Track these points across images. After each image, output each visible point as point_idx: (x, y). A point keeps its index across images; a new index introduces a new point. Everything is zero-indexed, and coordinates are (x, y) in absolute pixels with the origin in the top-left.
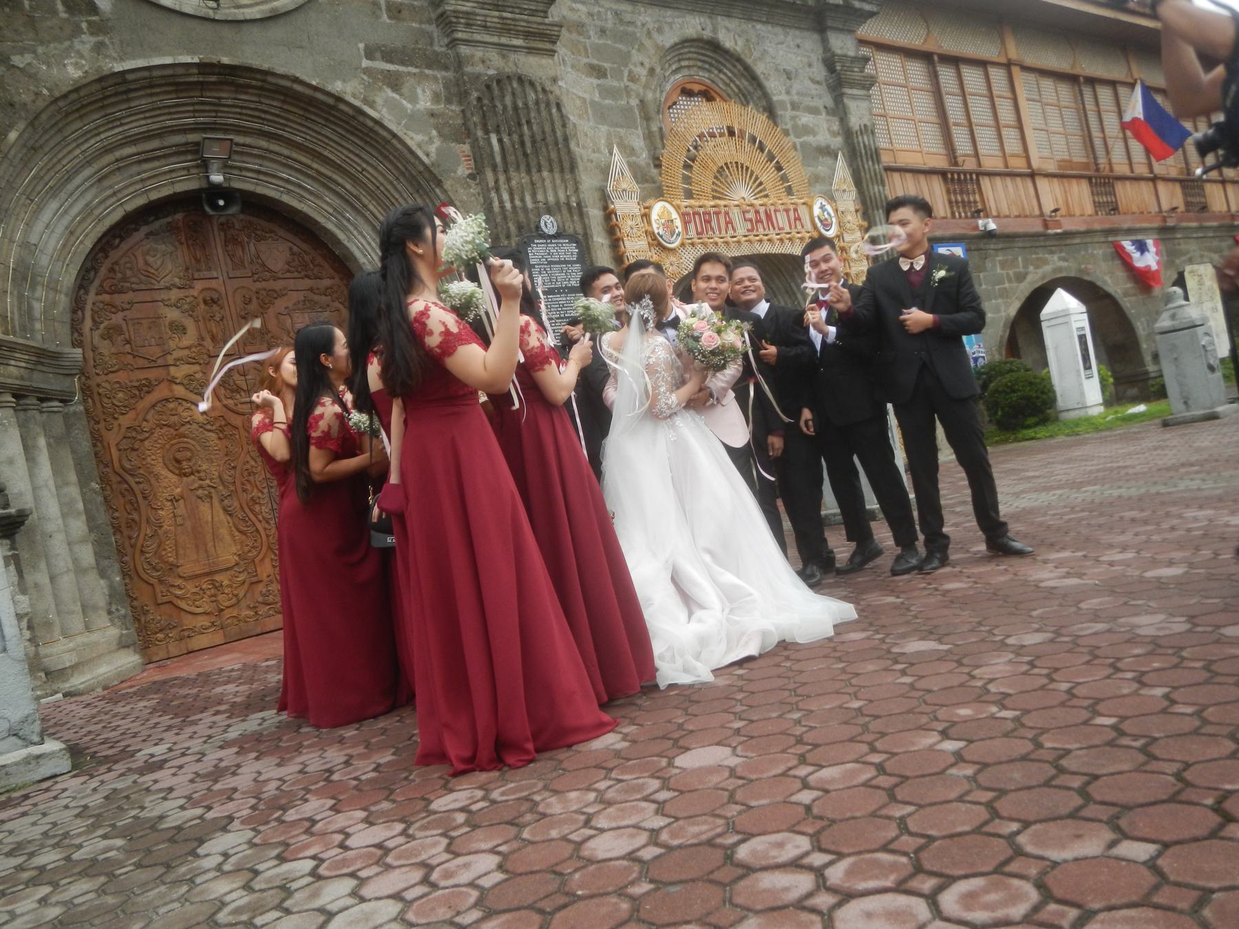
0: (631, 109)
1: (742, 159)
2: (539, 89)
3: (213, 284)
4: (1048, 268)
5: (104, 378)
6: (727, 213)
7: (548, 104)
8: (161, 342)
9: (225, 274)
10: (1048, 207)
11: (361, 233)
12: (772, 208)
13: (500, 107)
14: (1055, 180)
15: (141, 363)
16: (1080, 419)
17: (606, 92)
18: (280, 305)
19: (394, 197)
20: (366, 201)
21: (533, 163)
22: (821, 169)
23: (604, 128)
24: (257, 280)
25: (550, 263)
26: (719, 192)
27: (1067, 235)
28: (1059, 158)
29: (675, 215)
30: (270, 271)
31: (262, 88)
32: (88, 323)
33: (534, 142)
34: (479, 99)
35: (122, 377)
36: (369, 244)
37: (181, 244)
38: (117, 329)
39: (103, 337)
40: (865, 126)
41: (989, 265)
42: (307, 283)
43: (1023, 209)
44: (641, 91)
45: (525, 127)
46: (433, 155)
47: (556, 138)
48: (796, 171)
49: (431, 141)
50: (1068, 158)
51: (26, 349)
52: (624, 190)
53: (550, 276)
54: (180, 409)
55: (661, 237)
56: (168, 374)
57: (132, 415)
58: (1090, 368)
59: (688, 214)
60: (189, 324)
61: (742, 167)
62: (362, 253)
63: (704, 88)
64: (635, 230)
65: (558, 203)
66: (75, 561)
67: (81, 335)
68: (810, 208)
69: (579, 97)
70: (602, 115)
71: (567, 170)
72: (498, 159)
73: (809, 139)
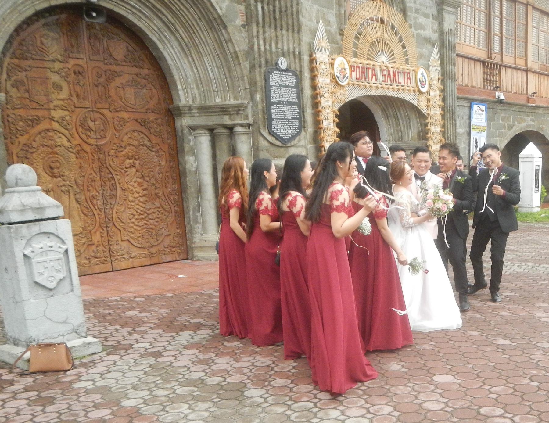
1: (386, 38)
3: (80, 62)
4: (524, 124)
5: (12, 111)
6: (374, 70)
8: (47, 95)
9: (88, 57)
10: (531, 91)
11: (172, 46)
12: (397, 70)
14: (537, 75)
15: (35, 105)
16: (528, 213)
18: (118, 81)
19: (196, 29)
21: (278, 25)
22: (425, 51)
23: (316, 7)
24: (106, 64)
25: (281, 86)
26: (371, 56)
27: (537, 107)
28: (540, 63)
29: (347, 67)
33: (280, 12)
35: (22, 112)
36: (176, 54)
37: (64, 34)
38: (22, 82)
39: (13, 86)
40: (451, 30)
41: (496, 118)
42: (135, 70)
43: (519, 89)
46: (224, 9)
47: (292, 11)
48: (412, 50)
50: (545, 63)
52: (322, 47)
53: (280, 93)
54: (56, 137)
56: (50, 115)
57: (26, 136)
58: (538, 187)
60: (64, 84)
61: (385, 43)
62: (171, 57)
65: (288, 50)
68: (416, 73)
71: (296, 32)
73: (421, 32)
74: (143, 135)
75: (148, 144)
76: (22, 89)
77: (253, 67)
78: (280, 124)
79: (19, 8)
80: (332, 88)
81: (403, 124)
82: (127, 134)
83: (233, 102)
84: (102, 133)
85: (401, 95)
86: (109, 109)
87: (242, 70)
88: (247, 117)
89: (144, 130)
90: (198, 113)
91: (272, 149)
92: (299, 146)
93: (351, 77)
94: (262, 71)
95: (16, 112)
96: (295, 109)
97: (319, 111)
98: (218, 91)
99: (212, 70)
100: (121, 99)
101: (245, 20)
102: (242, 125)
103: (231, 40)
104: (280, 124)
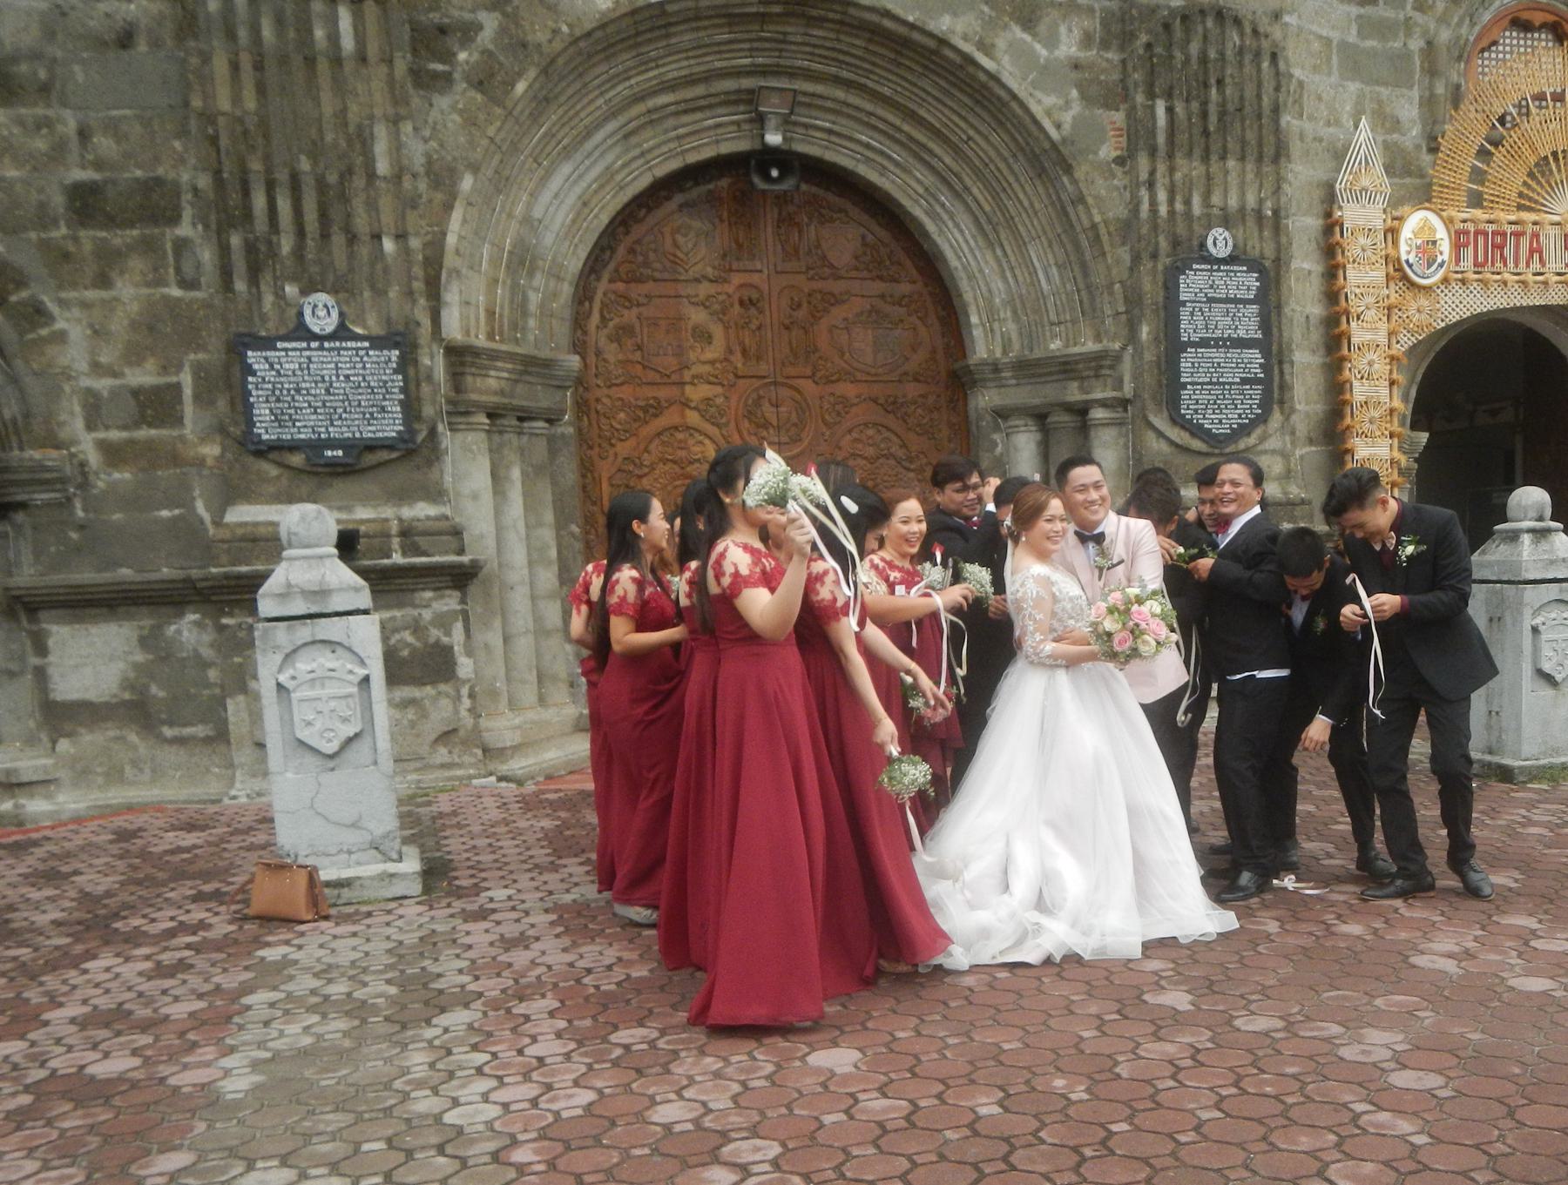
0: (1406, 56)
2: (1248, 30)
3: (755, 279)
5: (605, 391)
6: (1536, 236)
7: (1258, 55)
8: (680, 352)
13: (1179, 56)
15: (652, 376)
17: (1367, 27)
20: (968, 182)
21: (1215, 147)
23: (1353, 87)
24: (812, 278)
25: (1211, 300)
26: (1530, 199)
29: (1441, 234)
30: (832, 266)
32: (595, 318)
33: (1222, 114)
34: (1149, 46)
35: (625, 392)
37: (722, 221)
38: (627, 330)
39: (611, 339)
44: (1432, 26)
45: (1214, 91)
46: (1067, 127)
49: (1068, 105)
55: (1410, 266)
57: (632, 442)
59: (1467, 233)
60: (717, 331)
63: (1551, 18)
64: (1369, 253)
65: (1242, 209)
66: (538, 619)
67: (585, 333)
69: (1320, 37)
70: (1354, 63)
72: (1161, 139)
74: (887, 434)
75: (901, 453)
76: (629, 343)
77: (1136, 259)
80: (1393, 294)
82: (850, 431)
83: (1091, 346)
84: (793, 431)
86: (812, 377)
87: (1108, 268)
88: (1119, 384)
89: (890, 421)
90: (1013, 377)
93: (1458, 261)
94: (1160, 267)
95: (614, 392)
97: (1343, 359)
98: (1060, 323)
101: (1125, 145)
102: (1104, 404)
103: (1081, 199)
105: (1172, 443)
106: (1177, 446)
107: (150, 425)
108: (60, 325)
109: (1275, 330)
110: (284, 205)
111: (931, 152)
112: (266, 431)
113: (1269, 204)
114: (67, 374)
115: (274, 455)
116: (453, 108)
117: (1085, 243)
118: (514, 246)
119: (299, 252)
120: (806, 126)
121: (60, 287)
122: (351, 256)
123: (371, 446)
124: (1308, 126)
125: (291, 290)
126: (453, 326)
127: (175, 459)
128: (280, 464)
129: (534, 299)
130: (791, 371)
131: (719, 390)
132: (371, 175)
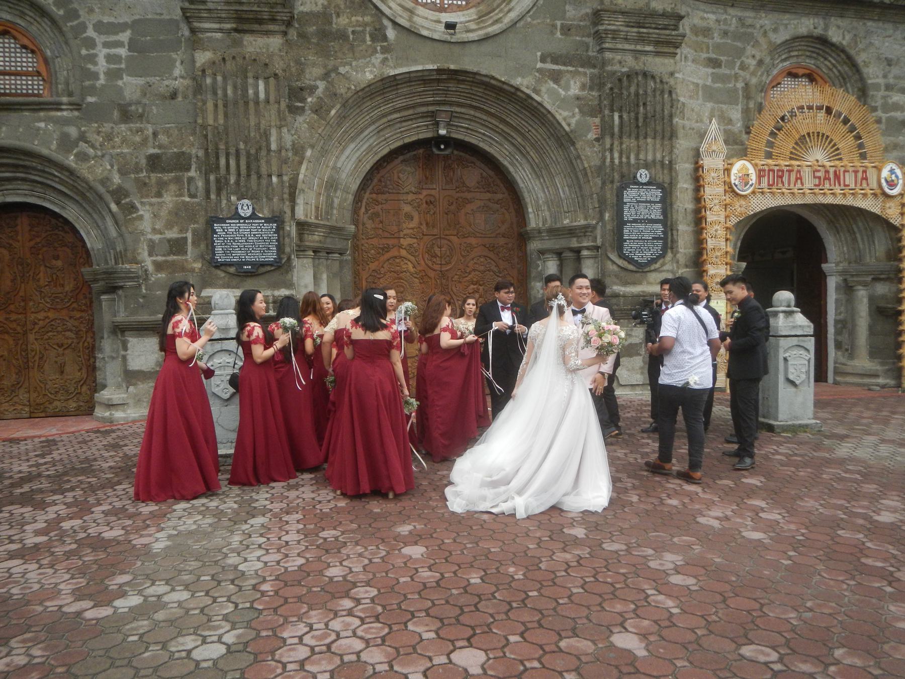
0: (735, 90)
2: (658, 81)
6: (799, 171)
7: (662, 92)
11: (523, 169)
13: (625, 93)
17: (716, 78)
21: (642, 132)
23: (709, 105)
25: (638, 202)
26: (796, 155)
29: (752, 171)
31: (473, 82)
33: (645, 118)
34: (611, 89)
44: (748, 77)
45: (642, 108)
46: (573, 125)
49: (574, 115)
51: (324, 226)
53: (636, 211)
59: (764, 170)
63: (808, 72)
65: (654, 161)
68: (879, 170)
69: (693, 83)
70: (709, 94)
72: (616, 130)
77: (604, 183)
78: (634, 246)
79: (374, 150)
81: (862, 239)
83: (583, 222)
85: (849, 201)
91: (623, 274)
92: (664, 271)
93: (760, 183)
96: (659, 228)
99: (563, 191)
100: (470, 226)
102: (588, 248)
103: (579, 157)
104: (634, 246)
105: (619, 266)
106: (622, 268)
107: (174, 254)
108: (141, 213)
109: (669, 215)
110: (232, 163)
111: (512, 136)
112: (220, 258)
113: (667, 158)
114: (142, 233)
115: (223, 268)
116: (305, 121)
117: (581, 177)
118: (328, 178)
119: (237, 183)
120: (457, 126)
121: (142, 197)
122: (259, 184)
123: (263, 264)
124: (686, 122)
125: (233, 198)
126: (300, 213)
127: (183, 269)
128: (225, 272)
129: (336, 201)
130: (447, 232)
131: (415, 240)
132: (269, 150)
